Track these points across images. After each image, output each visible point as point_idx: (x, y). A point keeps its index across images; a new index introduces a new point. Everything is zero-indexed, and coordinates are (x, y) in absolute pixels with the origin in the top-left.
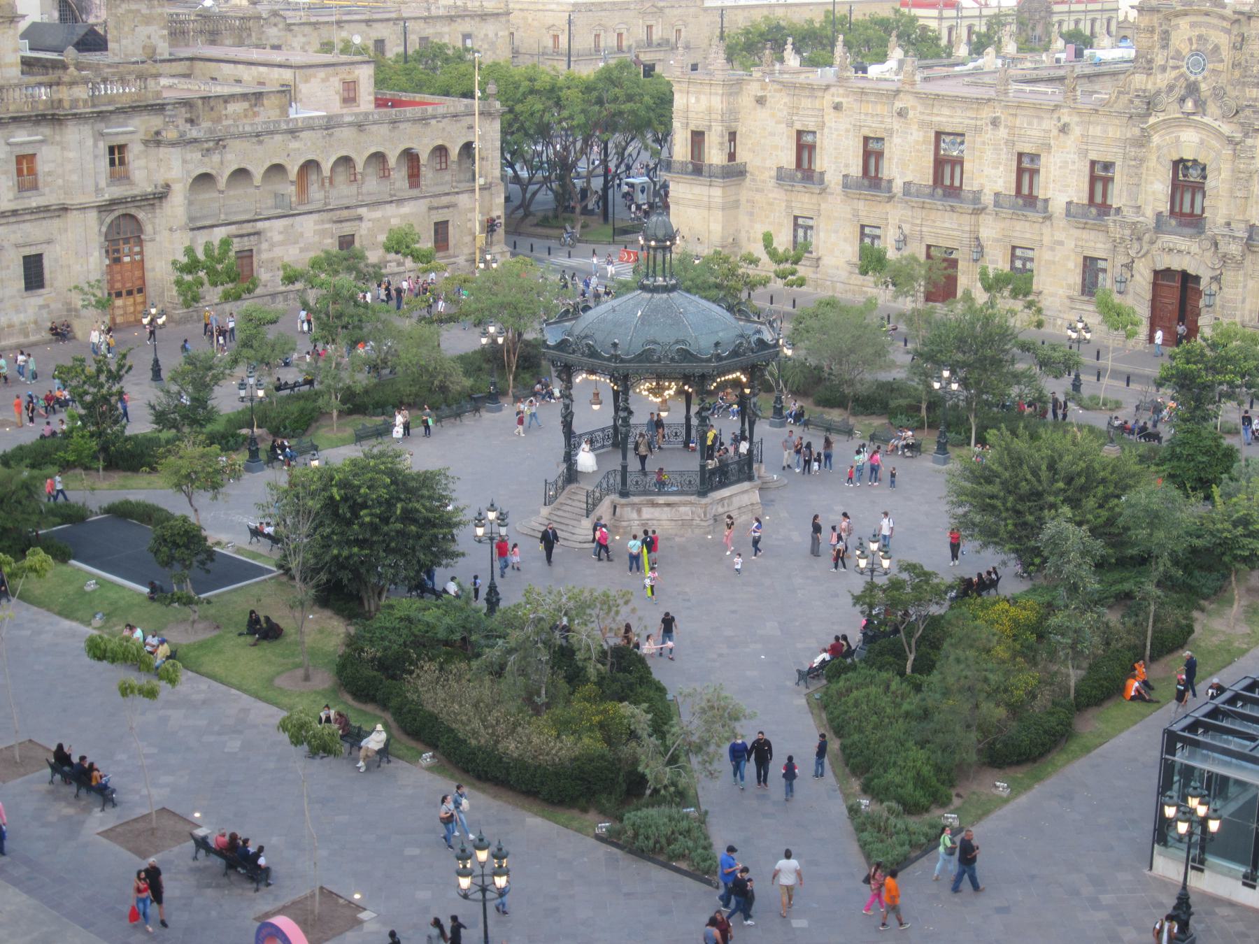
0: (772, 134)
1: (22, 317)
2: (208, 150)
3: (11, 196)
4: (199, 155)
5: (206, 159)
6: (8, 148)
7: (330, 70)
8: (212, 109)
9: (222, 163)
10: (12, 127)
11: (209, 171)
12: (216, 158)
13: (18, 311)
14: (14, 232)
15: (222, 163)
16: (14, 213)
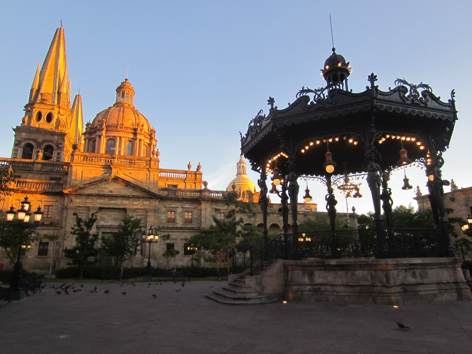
0: (460, 211)
1: (182, 263)
2: (250, 216)
3: (182, 224)
4: (247, 218)
5: (249, 219)
6: (182, 209)
7: (302, 205)
8: (255, 207)
9: (255, 221)
10: (184, 202)
11: (250, 223)
12: (253, 219)
13: (180, 261)
14: (182, 235)
15: (255, 221)
16: (181, 228)
